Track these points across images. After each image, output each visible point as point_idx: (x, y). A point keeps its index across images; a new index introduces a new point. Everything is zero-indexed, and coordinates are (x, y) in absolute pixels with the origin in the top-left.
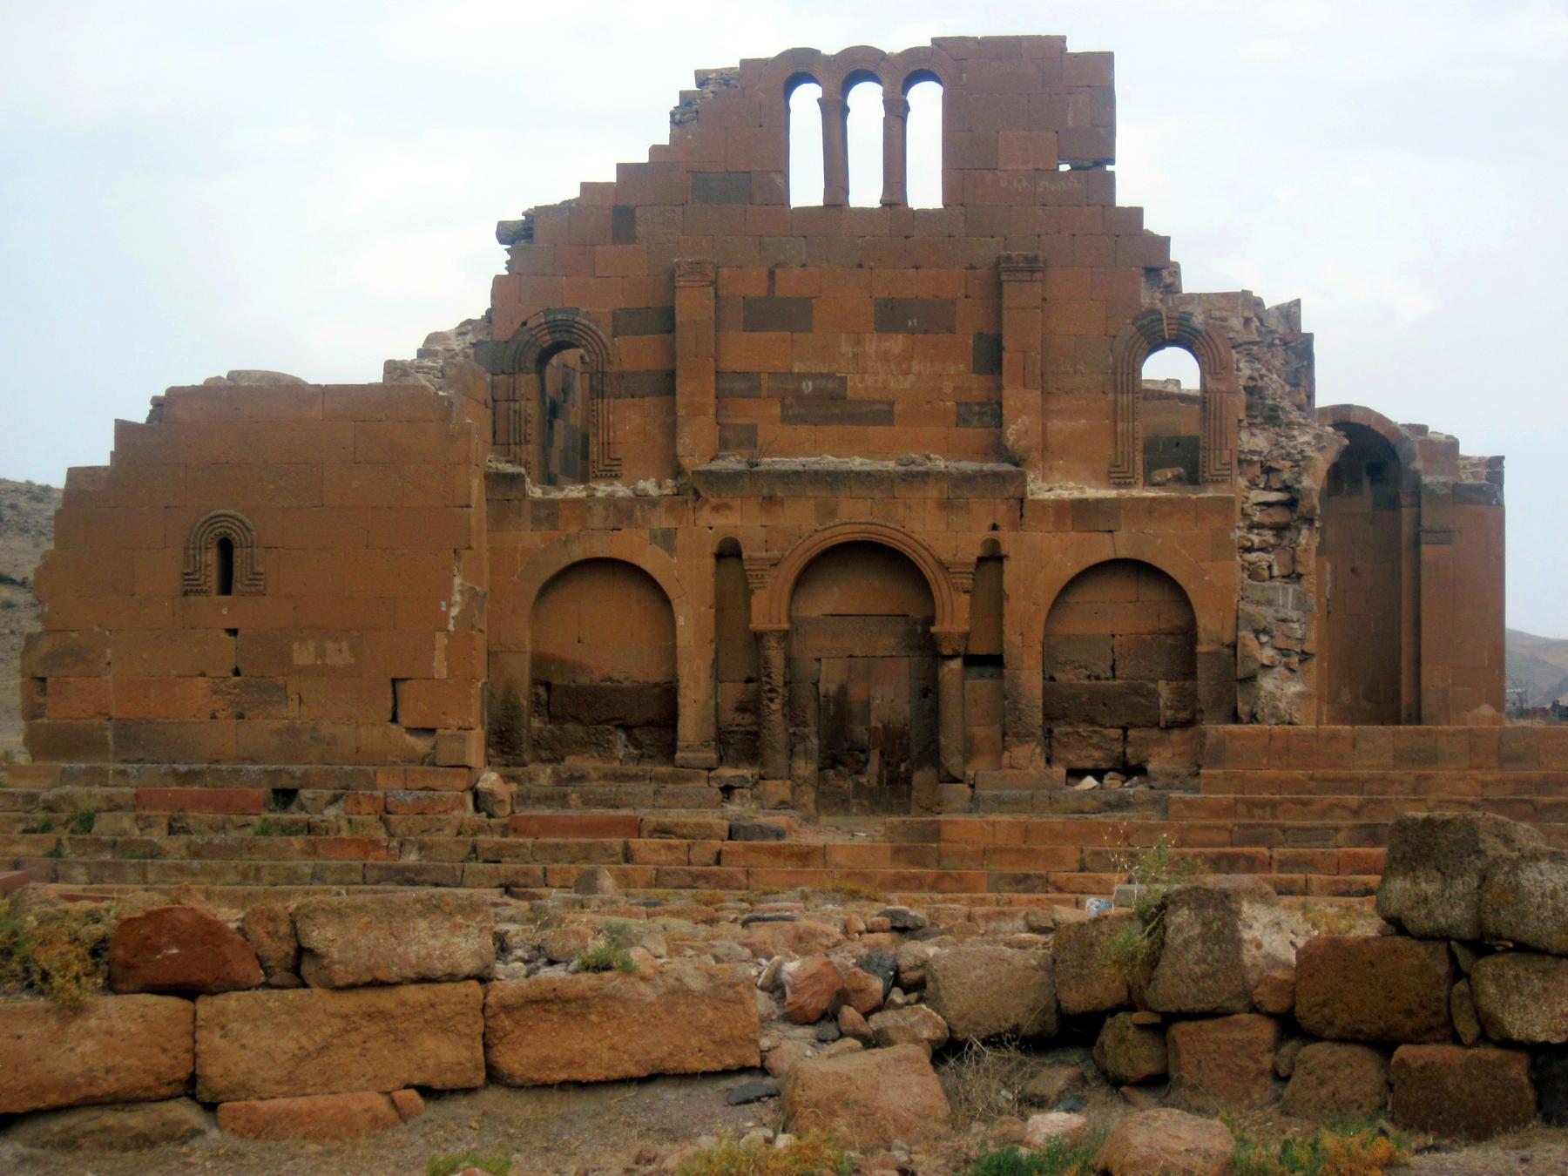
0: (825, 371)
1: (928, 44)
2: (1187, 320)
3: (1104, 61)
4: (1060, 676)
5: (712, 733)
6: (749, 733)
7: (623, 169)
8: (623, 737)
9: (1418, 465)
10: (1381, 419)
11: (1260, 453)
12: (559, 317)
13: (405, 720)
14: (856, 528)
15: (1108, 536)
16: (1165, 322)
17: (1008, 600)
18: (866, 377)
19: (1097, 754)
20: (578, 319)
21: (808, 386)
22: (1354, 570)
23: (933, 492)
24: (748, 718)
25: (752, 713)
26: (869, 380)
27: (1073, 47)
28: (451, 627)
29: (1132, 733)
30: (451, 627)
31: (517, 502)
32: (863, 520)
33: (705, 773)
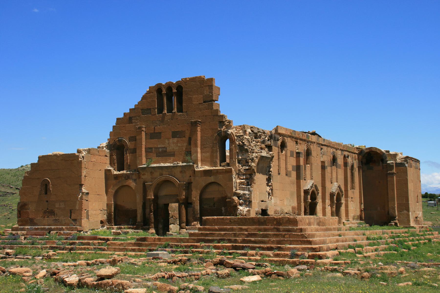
0: (163, 146)
1: (181, 80)
2: (226, 132)
3: (211, 80)
7: (130, 109)
8: (131, 220)
9: (388, 159)
10: (379, 150)
11: (245, 159)
12: (120, 139)
13: (72, 218)
18: (170, 147)
21: (161, 150)
22: (379, 182)
27: (206, 78)
28: (79, 199)
30: (79, 199)
33: (141, 227)
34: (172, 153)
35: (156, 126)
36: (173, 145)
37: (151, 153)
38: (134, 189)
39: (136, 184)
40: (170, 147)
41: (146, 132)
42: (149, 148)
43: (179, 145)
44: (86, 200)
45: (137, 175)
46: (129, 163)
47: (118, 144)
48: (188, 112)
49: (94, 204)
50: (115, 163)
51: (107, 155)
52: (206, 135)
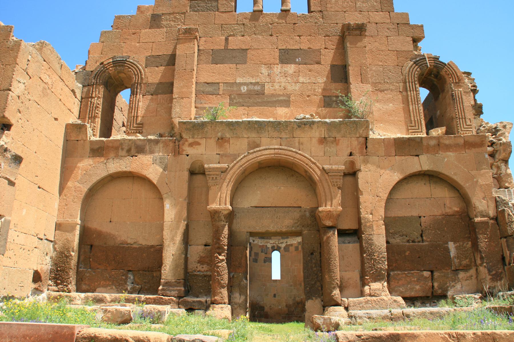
0: (254, 81)
4: (391, 241)
5: (182, 276)
6: (205, 276)
8: (132, 277)
14: (272, 151)
15: (417, 157)
16: (427, 59)
17: (362, 195)
18: (275, 84)
19: (418, 287)
20: (128, 60)
21: (244, 89)
23: (316, 133)
24: (205, 267)
25: (208, 264)
26: (277, 86)
29: (436, 274)
31: (82, 141)
32: (276, 147)
34: (281, 98)
35: (233, 35)
36: (283, 80)
37: (212, 95)
38: (155, 182)
39: (164, 170)
40: (275, 84)
41: (201, 48)
42: (208, 83)
43: (301, 79)
44: (6, 178)
45: (171, 144)
46: (139, 119)
47: (111, 70)
48: (325, 13)
49: (24, 212)
50: (95, 117)
51: (76, 91)
52: (381, 63)
